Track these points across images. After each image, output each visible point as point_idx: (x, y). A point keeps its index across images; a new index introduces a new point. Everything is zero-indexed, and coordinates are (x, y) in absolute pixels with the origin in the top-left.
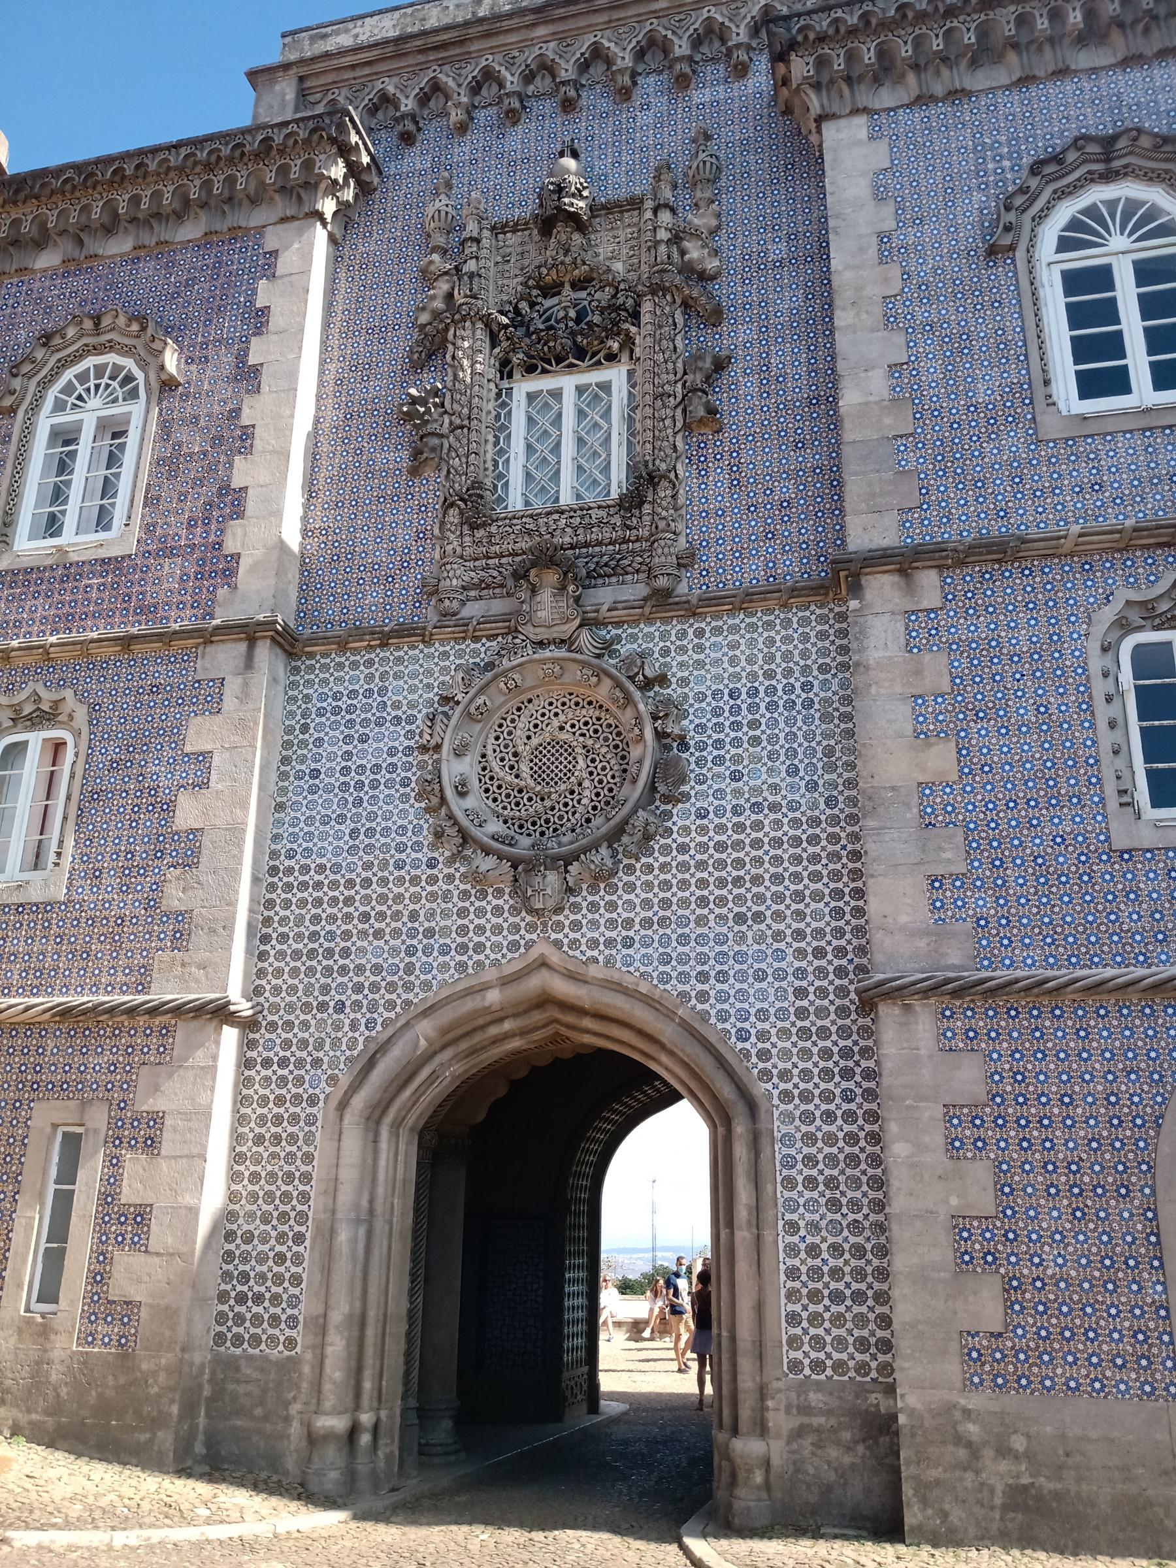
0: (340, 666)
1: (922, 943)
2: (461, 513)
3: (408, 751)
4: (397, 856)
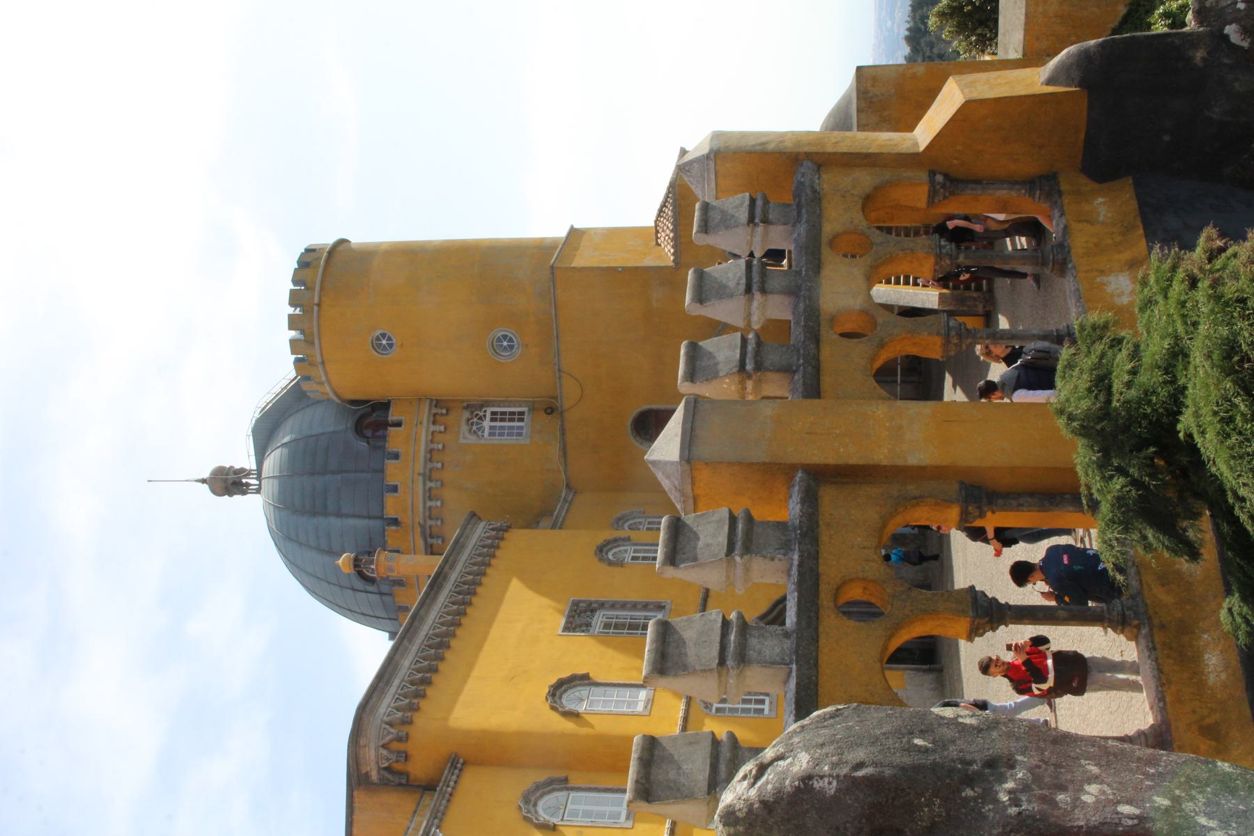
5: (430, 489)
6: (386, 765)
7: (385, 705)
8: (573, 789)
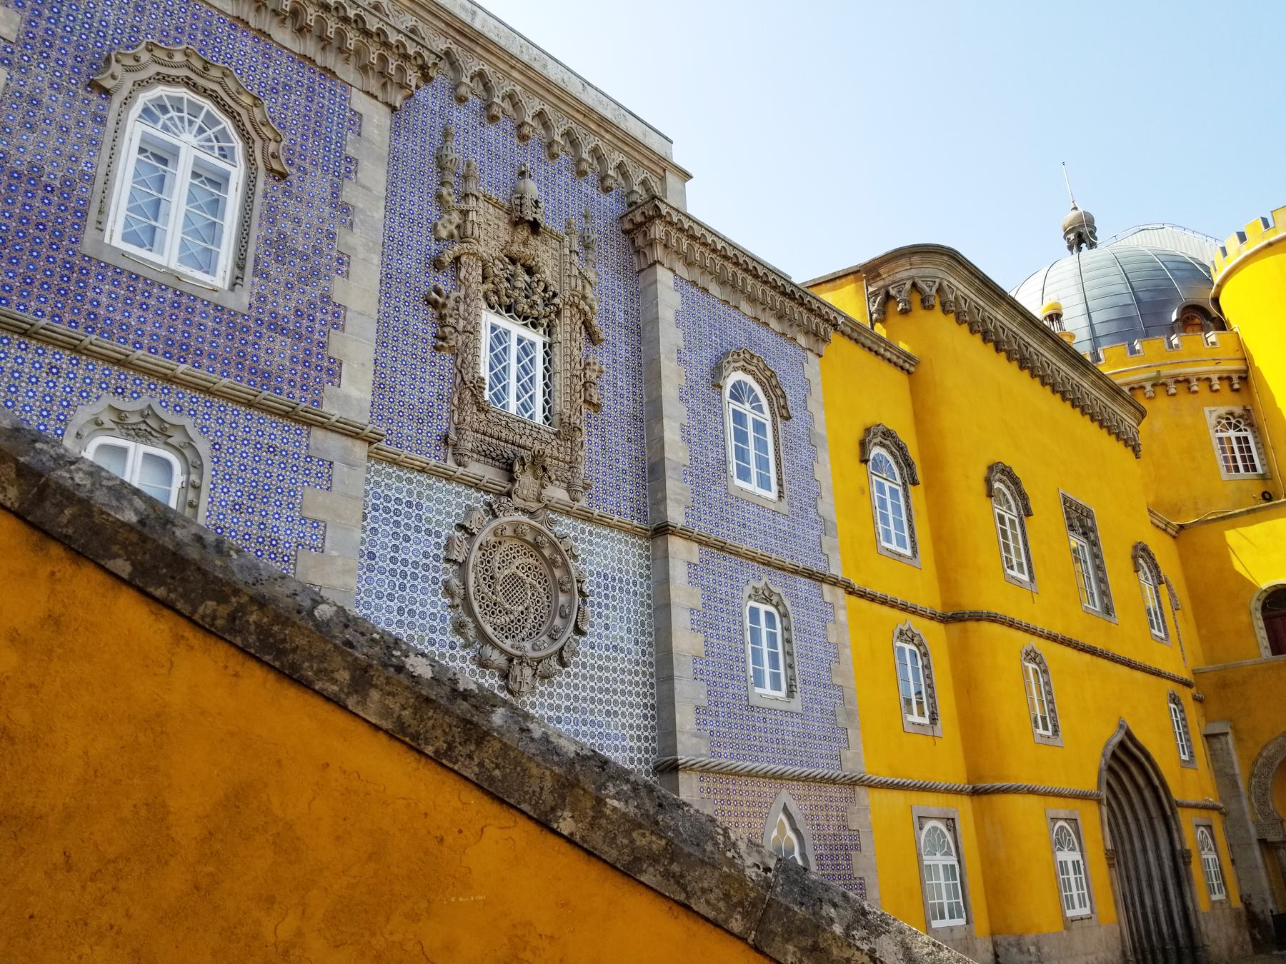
0: (389, 475)
1: (695, 740)
2: (473, 395)
3: (436, 557)
4: (431, 635)
5: (1143, 388)
6: (893, 292)
7: (960, 287)
8: (906, 490)
